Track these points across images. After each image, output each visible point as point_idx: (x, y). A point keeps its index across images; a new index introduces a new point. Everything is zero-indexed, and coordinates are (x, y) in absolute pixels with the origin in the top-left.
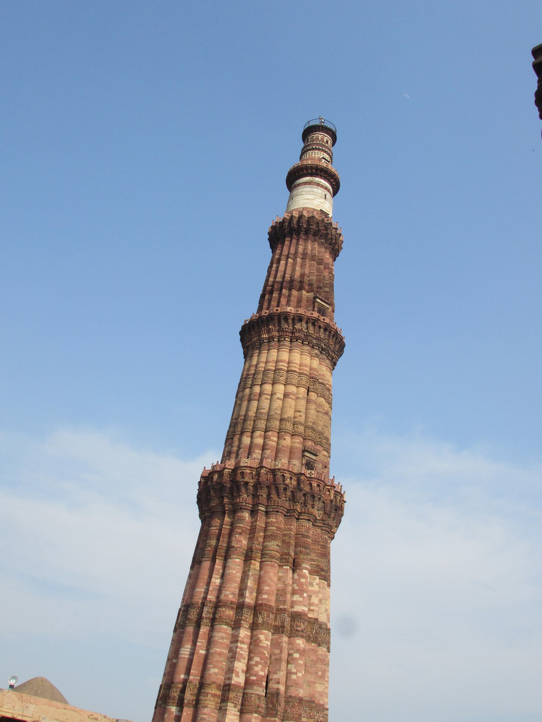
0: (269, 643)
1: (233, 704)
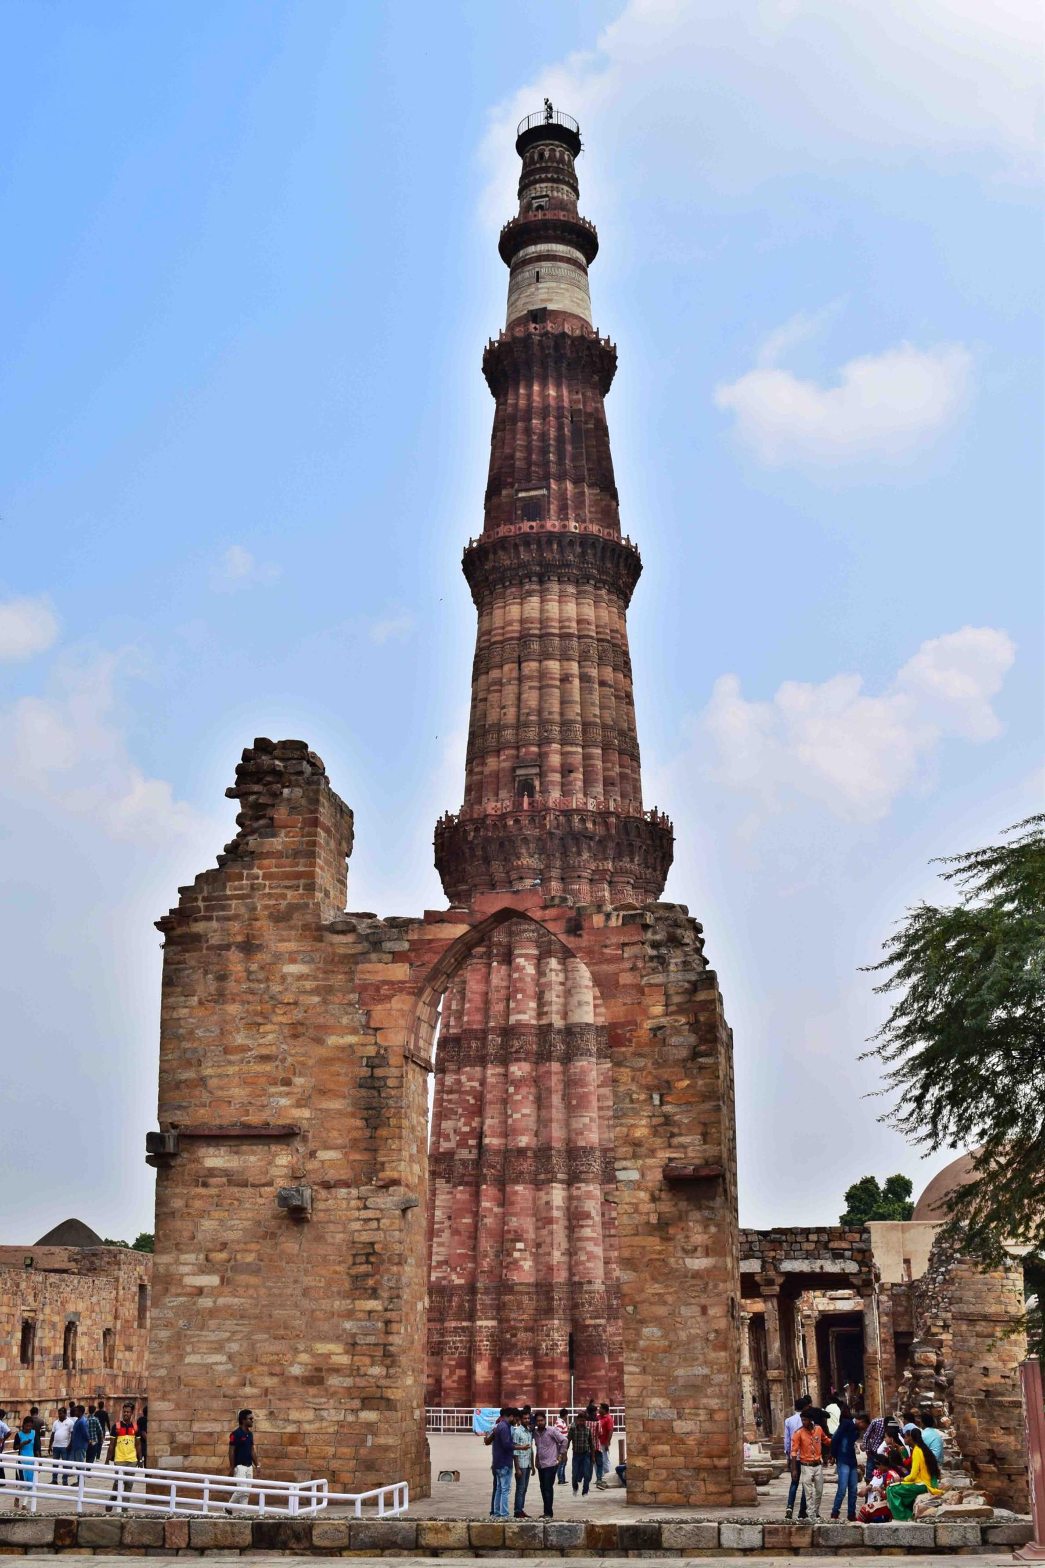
0: (476, 1084)
1: (443, 1180)
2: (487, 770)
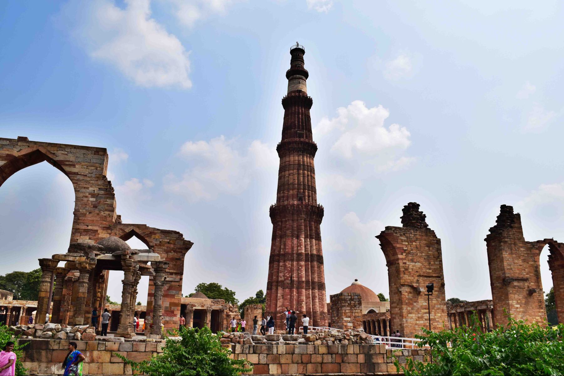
2: (290, 193)
